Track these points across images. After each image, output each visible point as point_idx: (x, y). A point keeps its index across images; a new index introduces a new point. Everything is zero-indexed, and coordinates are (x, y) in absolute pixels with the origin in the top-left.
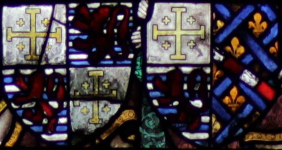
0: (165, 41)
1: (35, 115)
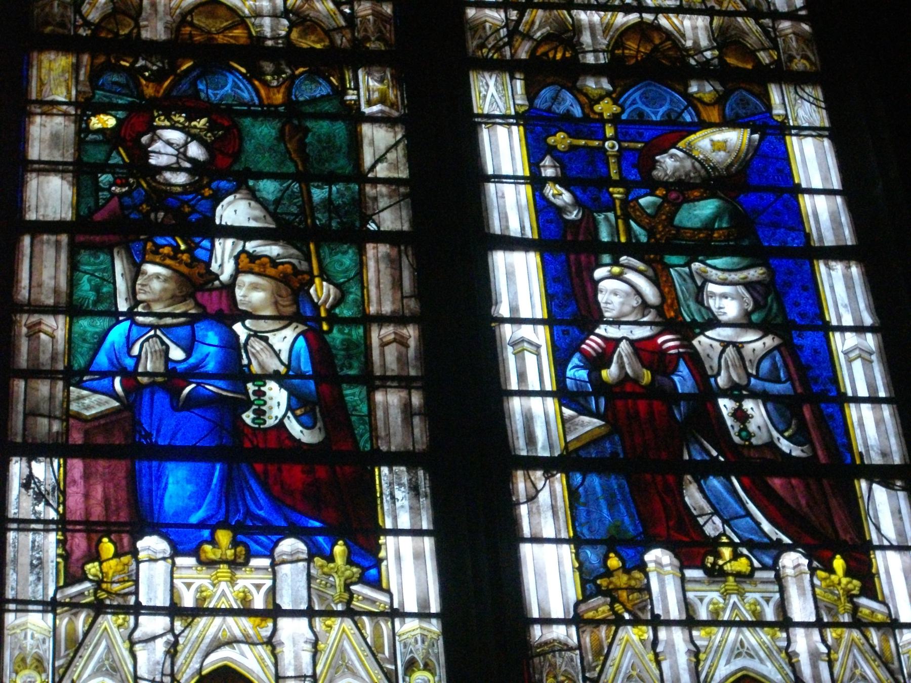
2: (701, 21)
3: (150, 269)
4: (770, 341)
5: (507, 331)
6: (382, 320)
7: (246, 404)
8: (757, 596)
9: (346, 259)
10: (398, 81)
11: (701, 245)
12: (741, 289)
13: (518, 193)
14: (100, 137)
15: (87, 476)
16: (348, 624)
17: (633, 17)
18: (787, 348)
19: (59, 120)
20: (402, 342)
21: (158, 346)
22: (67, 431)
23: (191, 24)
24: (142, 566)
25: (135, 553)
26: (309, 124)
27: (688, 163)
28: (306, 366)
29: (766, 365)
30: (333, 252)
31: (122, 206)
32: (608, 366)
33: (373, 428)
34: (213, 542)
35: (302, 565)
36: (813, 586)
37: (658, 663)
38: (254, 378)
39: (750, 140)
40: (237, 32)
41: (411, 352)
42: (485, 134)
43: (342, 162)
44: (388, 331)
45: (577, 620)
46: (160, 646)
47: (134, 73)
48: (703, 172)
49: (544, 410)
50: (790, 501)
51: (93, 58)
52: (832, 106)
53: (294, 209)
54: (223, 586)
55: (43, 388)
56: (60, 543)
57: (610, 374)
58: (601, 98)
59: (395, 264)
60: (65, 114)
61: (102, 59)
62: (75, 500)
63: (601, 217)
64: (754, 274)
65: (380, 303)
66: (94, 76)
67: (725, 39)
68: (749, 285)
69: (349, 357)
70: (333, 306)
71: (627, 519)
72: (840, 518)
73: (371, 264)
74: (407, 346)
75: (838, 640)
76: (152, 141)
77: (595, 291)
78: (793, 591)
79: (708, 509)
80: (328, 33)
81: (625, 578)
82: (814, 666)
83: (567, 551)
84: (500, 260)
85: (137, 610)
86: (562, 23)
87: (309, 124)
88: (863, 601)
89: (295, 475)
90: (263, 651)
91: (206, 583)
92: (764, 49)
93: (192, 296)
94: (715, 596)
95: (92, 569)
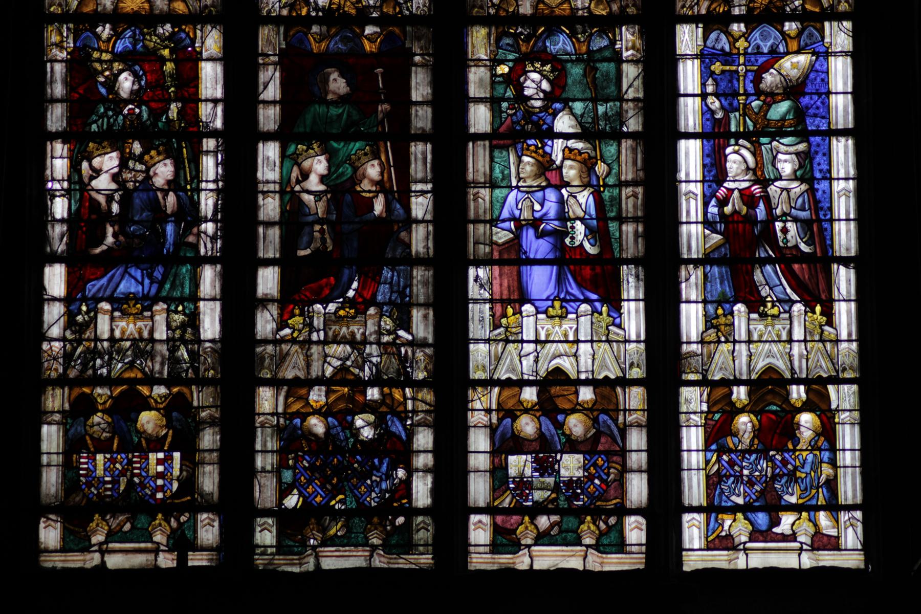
0: (567, 468)
1: (521, 496)
3: (526, 159)
4: (804, 187)
5: (683, 187)
6: (627, 184)
7: (568, 233)
8: (780, 326)
9: (612, 149)
11: (778, 131)
12: (794, 156)
13: (694, 103)
14: (501, 79)
15: (501, 275)
16: (607, 346)
18: (812, 191)
19: (482, 69)
20: (635, 195)
21: (529, 204)
22: (492, 252)
24: (525, 319)
25: (521, 313)
26: (598, 65)
27: (778, 78)
28: (593, 212)
29: (800, 201)
30: (607, 145)
31: (513, 122)
32: (727, 205)
33: (621, 245)
34: (553, 307)
35: (589, 317)
36: (805, 320)
37: (734, 361)
38: (570, 219)
39: (811, 61)
40: (565, 6)
41: (640, 202)
42: (681, 66)
43: (613, 88)
44: (629, 190)
45: (702, 342)
46: (532, 357)
47: (516, 36)
48: (785, 83)
49: (696, 230)
50: (801, 276)
51: (497, 28)
52: (856, 35)
53: (590, 120)
54: (557, 328)
55: (481, 228)
56: (491, 309)
57: (728, 209)
58: (740, 37)
59: (634, 151)
60: (485, 66)
61: (500, 30)
62: (496, 288)
63: (732, 115)
64: (802, 147)
65: (627, 174)
66: (498, 40)
68: (797, 154)
69: (612, 206)
70: (606, 177)
71: (728, 289)
72: (822, 285)
73: (624, 151)
74: (637, 198)
75: (812, 348)
76: (525, 80)
77: (726, 161)
78: (796, 324)
79: (764, 282)
81: (724, 319)
82: (800, 362)
83: (700, 306)
84: (683, 144)
85: (522, 341)
87: (598, 65)
88: (827, 328)
89: (587, 271)
90: (572, 359)
91: (550, 326)
94: (761, 327)
95: (504, 321)
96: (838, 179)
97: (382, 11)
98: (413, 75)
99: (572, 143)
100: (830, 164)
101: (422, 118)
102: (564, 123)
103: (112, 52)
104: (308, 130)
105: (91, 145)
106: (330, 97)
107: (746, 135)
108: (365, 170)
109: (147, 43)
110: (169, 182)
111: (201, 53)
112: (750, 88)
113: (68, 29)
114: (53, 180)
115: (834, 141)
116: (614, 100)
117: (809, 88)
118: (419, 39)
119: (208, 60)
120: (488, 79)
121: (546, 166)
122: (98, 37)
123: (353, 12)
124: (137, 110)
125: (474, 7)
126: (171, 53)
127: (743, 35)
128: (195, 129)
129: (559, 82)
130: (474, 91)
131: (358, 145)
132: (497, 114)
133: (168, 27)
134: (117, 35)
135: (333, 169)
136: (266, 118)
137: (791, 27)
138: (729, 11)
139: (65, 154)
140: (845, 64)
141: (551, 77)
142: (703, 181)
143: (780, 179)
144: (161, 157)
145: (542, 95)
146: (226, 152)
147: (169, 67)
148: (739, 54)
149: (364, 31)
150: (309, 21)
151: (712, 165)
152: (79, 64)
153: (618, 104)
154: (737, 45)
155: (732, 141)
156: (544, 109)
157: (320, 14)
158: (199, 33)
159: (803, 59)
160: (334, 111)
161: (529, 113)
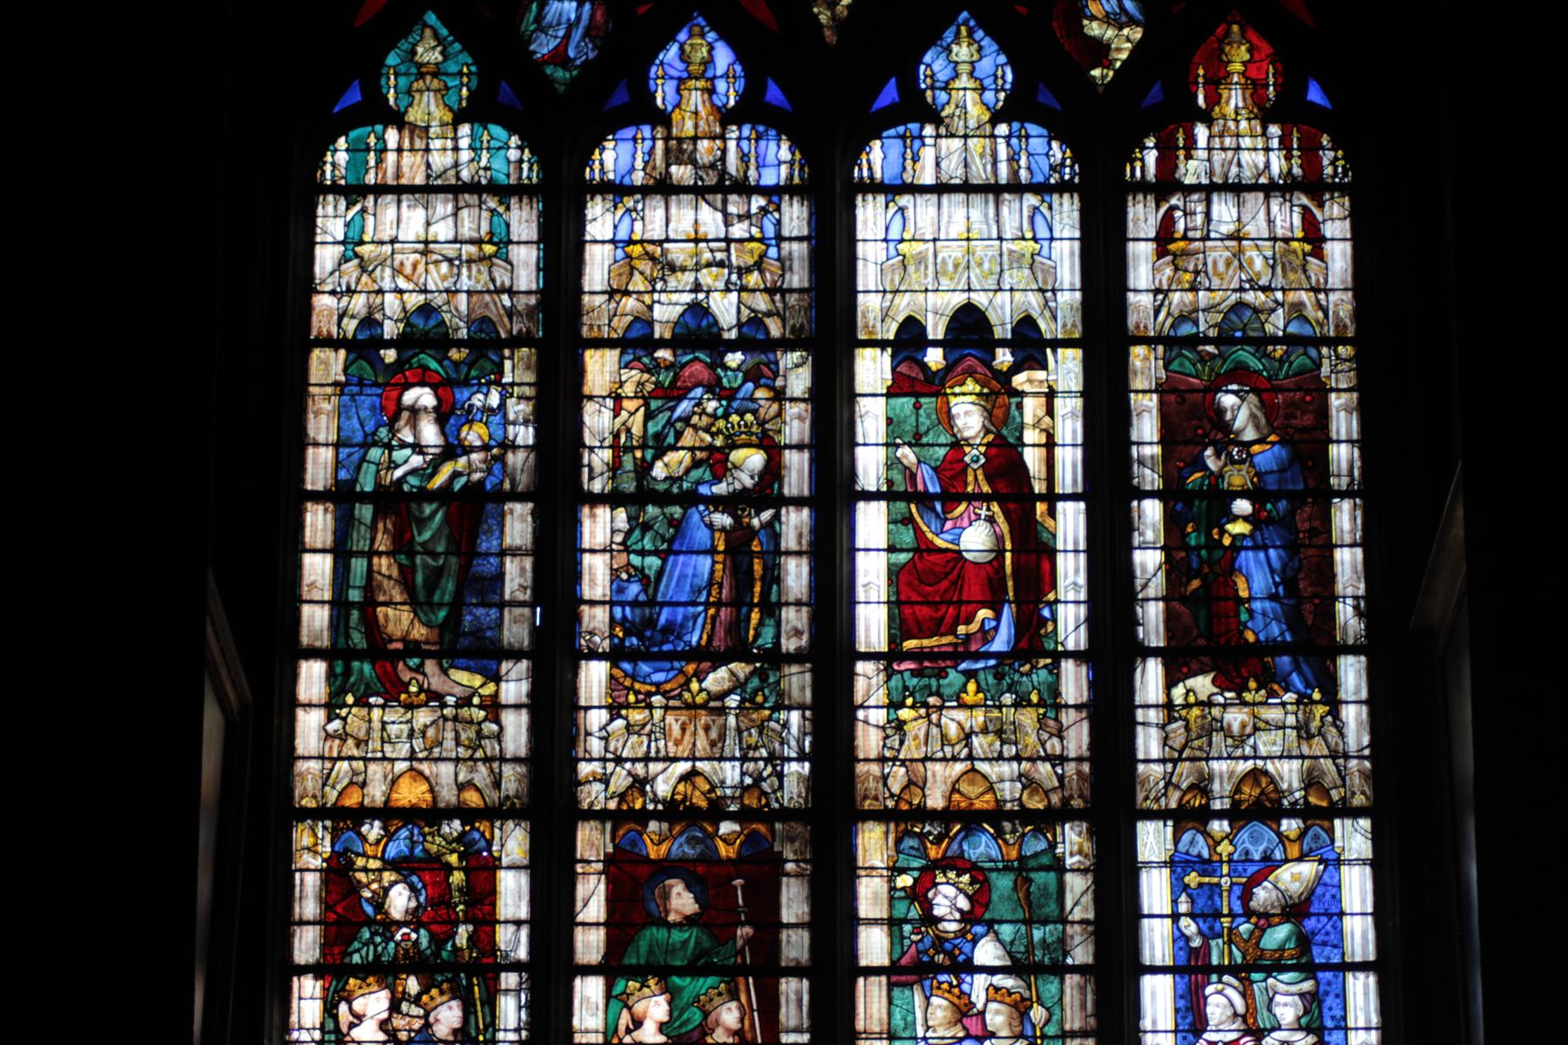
2: (1296, 764)
10: (1091, 833)
11: (1275, 966)
14: (902, 894)
17: (1250, 764)
19: (878, 880)
23: (959, 791)
27: (1274, 893)
31: (919, 952)
40: (988, 797)
47: (922, 837)
51: (897, 826)
52: (1377, 837)
59: (1083, 990)
61: (902, 827)
63: (1213, 943)
64: (1307, 986)
66: (898, 841)
67: (1311, 781)
68: (1302, 995)
73: (1068, 991)
80: (1046, 793)
86: (1201, 773)
92: (1336, 787)
93: (960, 1021)
96: (1357, 1029)
97: (742, 803)
98: (784, 888)
99: (999, 980)
100: (1345, 1009)
101: (796, 946)
102: (987, 952)
103: (382, 859)
104: (642, 961)
105: (352, 981)
106: (672, 918)
107: (1233, 970)
108: (719, 1015)
109: (428, 845)
110: (455, 1032)
111: (499, 859)
112: (1238, 908)
113: (325, 828)
114: (300, 1028)
115: (1349, 976)
116: (1055, 922)
117: (1315, 908)
118: (792, 840)
119: (509, 868)
120: (885, 895)
121: (963, 1011)
122: (364, 839)
123: (703, 804)
124: (414, 936)
125: (866, 797)
126: (460, 859)
127: (1227, 836)
128: (491, 960)
129: (980, 898)
130: (865, 909)
131: (711, 980)
132: (896, 941)
133: (457, 824)
134: (389, 836)
135: (676, 1014)
136: (587, 945)
137: (1290, 826)
138: (1208, 804)
139: (318, 992)
140: (1362, 875)
141: (970, 891)
142: (1176, 1031)
143: (1279, 1028)
144: (445, 998)
145: (958, 916)
146: (532, 990)
147: (457, 878)
148: (1221, 862)
149: (718, 829)
150: (643, 816)
151: (1187, 1009)
152: (338, 874)
153: (1060, 927)
154: (1219, 849)
155: (1214, 978)
156: (962, 933)
157: (660, 807)
158: (497, 832)
159: (1308, 869)
160: (677, 936)
161: (940, 942)
